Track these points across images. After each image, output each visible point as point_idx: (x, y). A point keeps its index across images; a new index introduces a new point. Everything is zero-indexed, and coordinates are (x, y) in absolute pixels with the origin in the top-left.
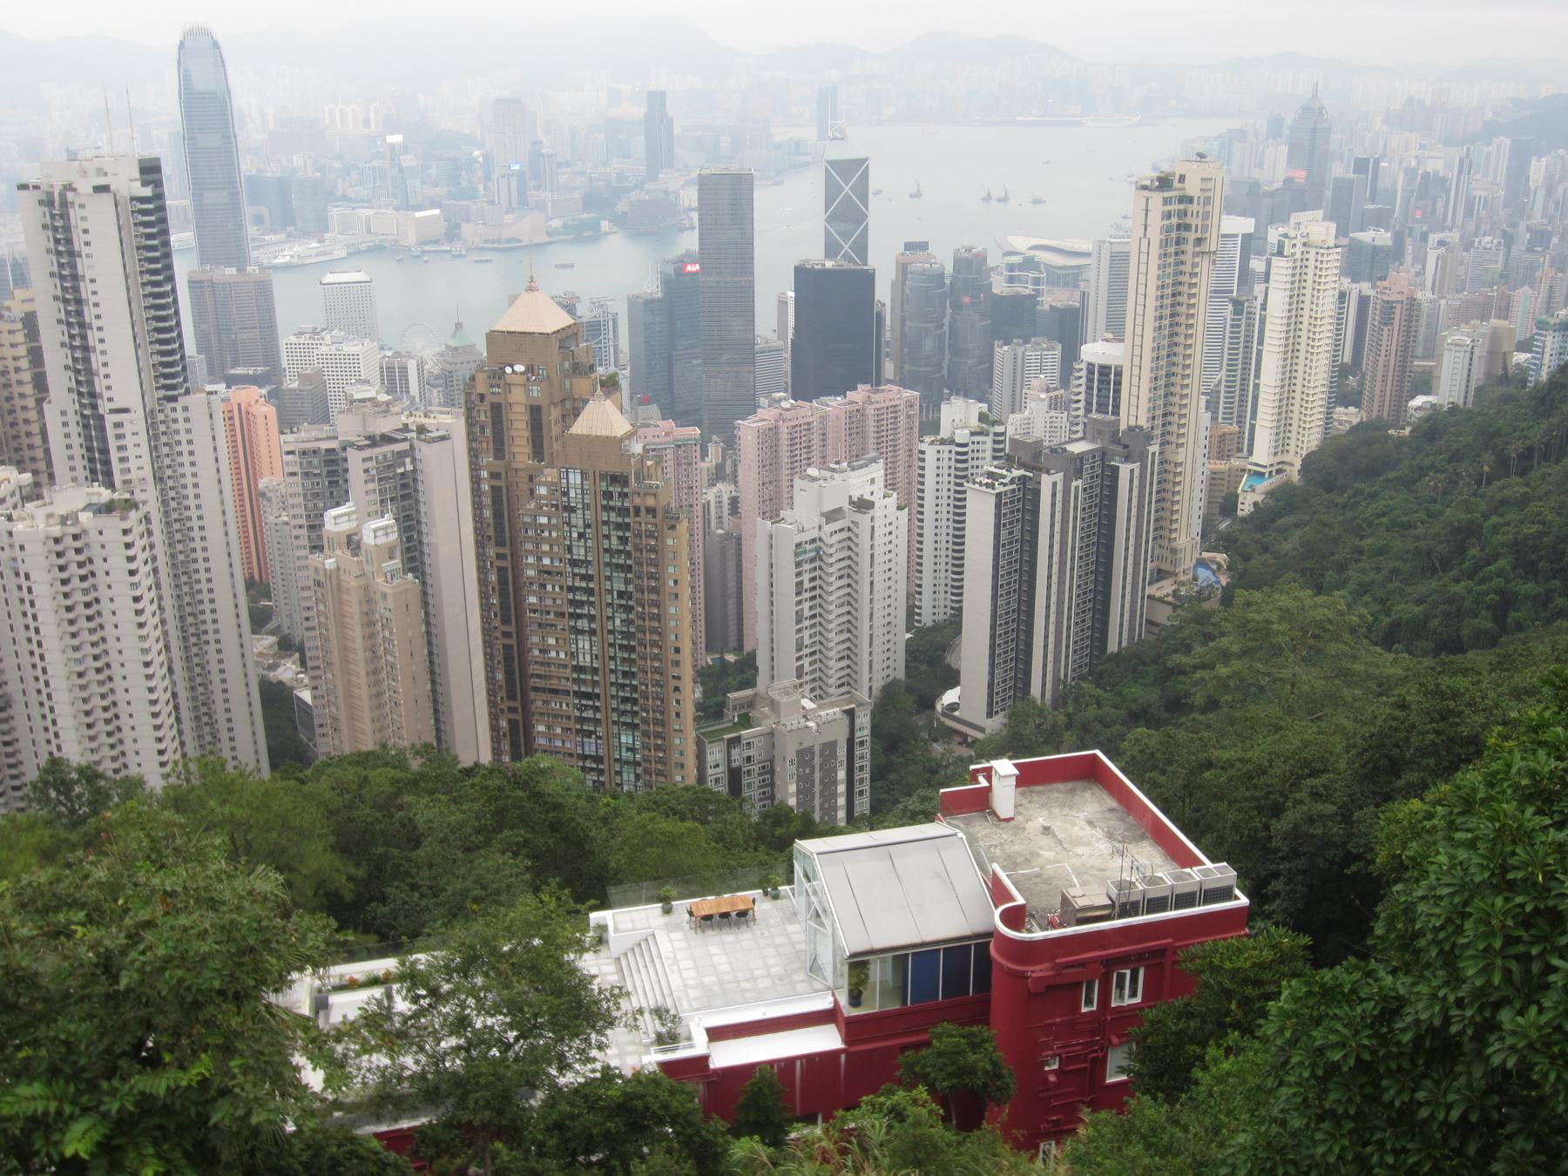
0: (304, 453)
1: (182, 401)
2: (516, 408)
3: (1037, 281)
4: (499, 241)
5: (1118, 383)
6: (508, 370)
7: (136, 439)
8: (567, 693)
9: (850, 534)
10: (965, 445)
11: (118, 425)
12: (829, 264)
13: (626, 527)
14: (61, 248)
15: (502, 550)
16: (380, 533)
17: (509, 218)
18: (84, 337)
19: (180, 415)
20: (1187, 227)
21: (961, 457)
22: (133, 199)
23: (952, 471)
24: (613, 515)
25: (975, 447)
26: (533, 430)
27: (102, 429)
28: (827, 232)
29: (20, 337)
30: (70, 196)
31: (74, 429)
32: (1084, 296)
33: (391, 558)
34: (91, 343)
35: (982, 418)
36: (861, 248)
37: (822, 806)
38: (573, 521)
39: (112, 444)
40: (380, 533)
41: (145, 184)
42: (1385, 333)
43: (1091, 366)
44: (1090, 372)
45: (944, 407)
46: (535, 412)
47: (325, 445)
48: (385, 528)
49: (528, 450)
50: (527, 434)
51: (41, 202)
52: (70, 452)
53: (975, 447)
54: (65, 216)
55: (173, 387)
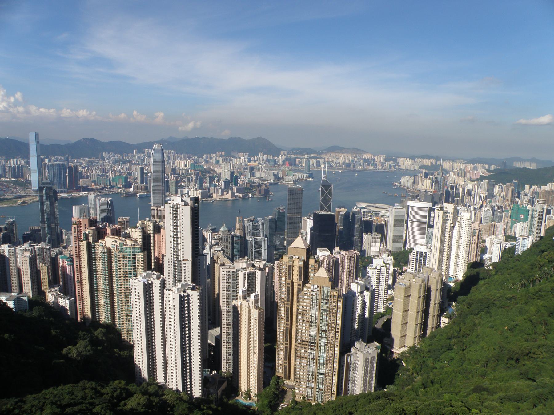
0: (227, 272)
1: (199, 257)
2: (295, 267)
3: (371, 216)
4: (223, 198)
5: (425, 257)
6: (294, 257)
8: (307, 342)
11: (185, 264)
12: (323, 212)
13: (328, 300)
14: (174, 219)
15: (288, 303)
18: (177, 241)
20: (448, 220)
21: (380, 273)
23: (376, 276)
27: (181, 264)
29: (140, 234)
30: (179, 206)
31: (171, 263)
32: (387, 222)
34: (179, 242)
35: (384, 262)
37: (370, 373)
38: (314, 298)
39: (183, 268)
42: (474, 238)
43: (417, 252)
44: (417, 252)
45: (374, 259)
46: (300, 268)
47: (233, 270)
49: (298, 277)
50: (298, 273)
51: (170, 207)
52: (169, 269)
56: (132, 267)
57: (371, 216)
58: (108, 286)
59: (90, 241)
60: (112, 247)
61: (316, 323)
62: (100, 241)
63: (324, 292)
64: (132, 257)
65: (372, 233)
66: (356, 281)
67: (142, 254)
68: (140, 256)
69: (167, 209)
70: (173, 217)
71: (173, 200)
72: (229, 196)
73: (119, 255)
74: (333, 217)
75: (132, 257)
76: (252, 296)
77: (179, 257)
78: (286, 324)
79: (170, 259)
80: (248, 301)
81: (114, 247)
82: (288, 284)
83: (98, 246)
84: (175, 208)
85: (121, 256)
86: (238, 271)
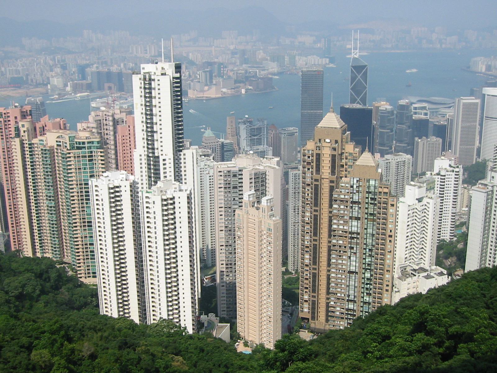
1: (184, 151)
3: (426, 114)
4: (203, 97)
7: (170, 165)
9: (426, 207)
10: (445, 176)
11: (164, 160)
16: (269, 201)
17: (206, 88)
19: (182, 157)
21: (443, 181)
22: (173, 78)
24: (370, 195)
25: (448, 177)
26: (332, 163)
28: (351, 94)
30: (153, 77)
31: (144, 161)
33: (272, 210)
36: (364, 101)
39: (162, 167)
40: (269, 201)
41: (176, 72)
48: (270, 199)
49: (329, 171)
50: (330, 165)
53: (448, 177)
54: (150, 84)
55: (181, 146)
56: (88, 170)
57: (426, 114)
58: (53, 202)
59: (23, 138)
60: (58, 145)
61: (358, 234)
62: (40, 138)
63: (369, 187)
64: (87, 155)
65: (427, 137)
66: (412, 183)
67: (102, 150)
68: (99, 154)
69: (137, 82)
70: (145, 93)
71: (143, 68)
72: (212, 93)
73: (69, 153)
74: (370, 111)
75: (87, 155)
76: (264, 200)
77: (156, 151)
78: (314, 240)
79: (143, 155)
80: (258, 209)
81: (60, 146)
82: (316, 180)
83: (36, 145)
84: (148, 81)
85: (71, 155)
86: (240, 171)
